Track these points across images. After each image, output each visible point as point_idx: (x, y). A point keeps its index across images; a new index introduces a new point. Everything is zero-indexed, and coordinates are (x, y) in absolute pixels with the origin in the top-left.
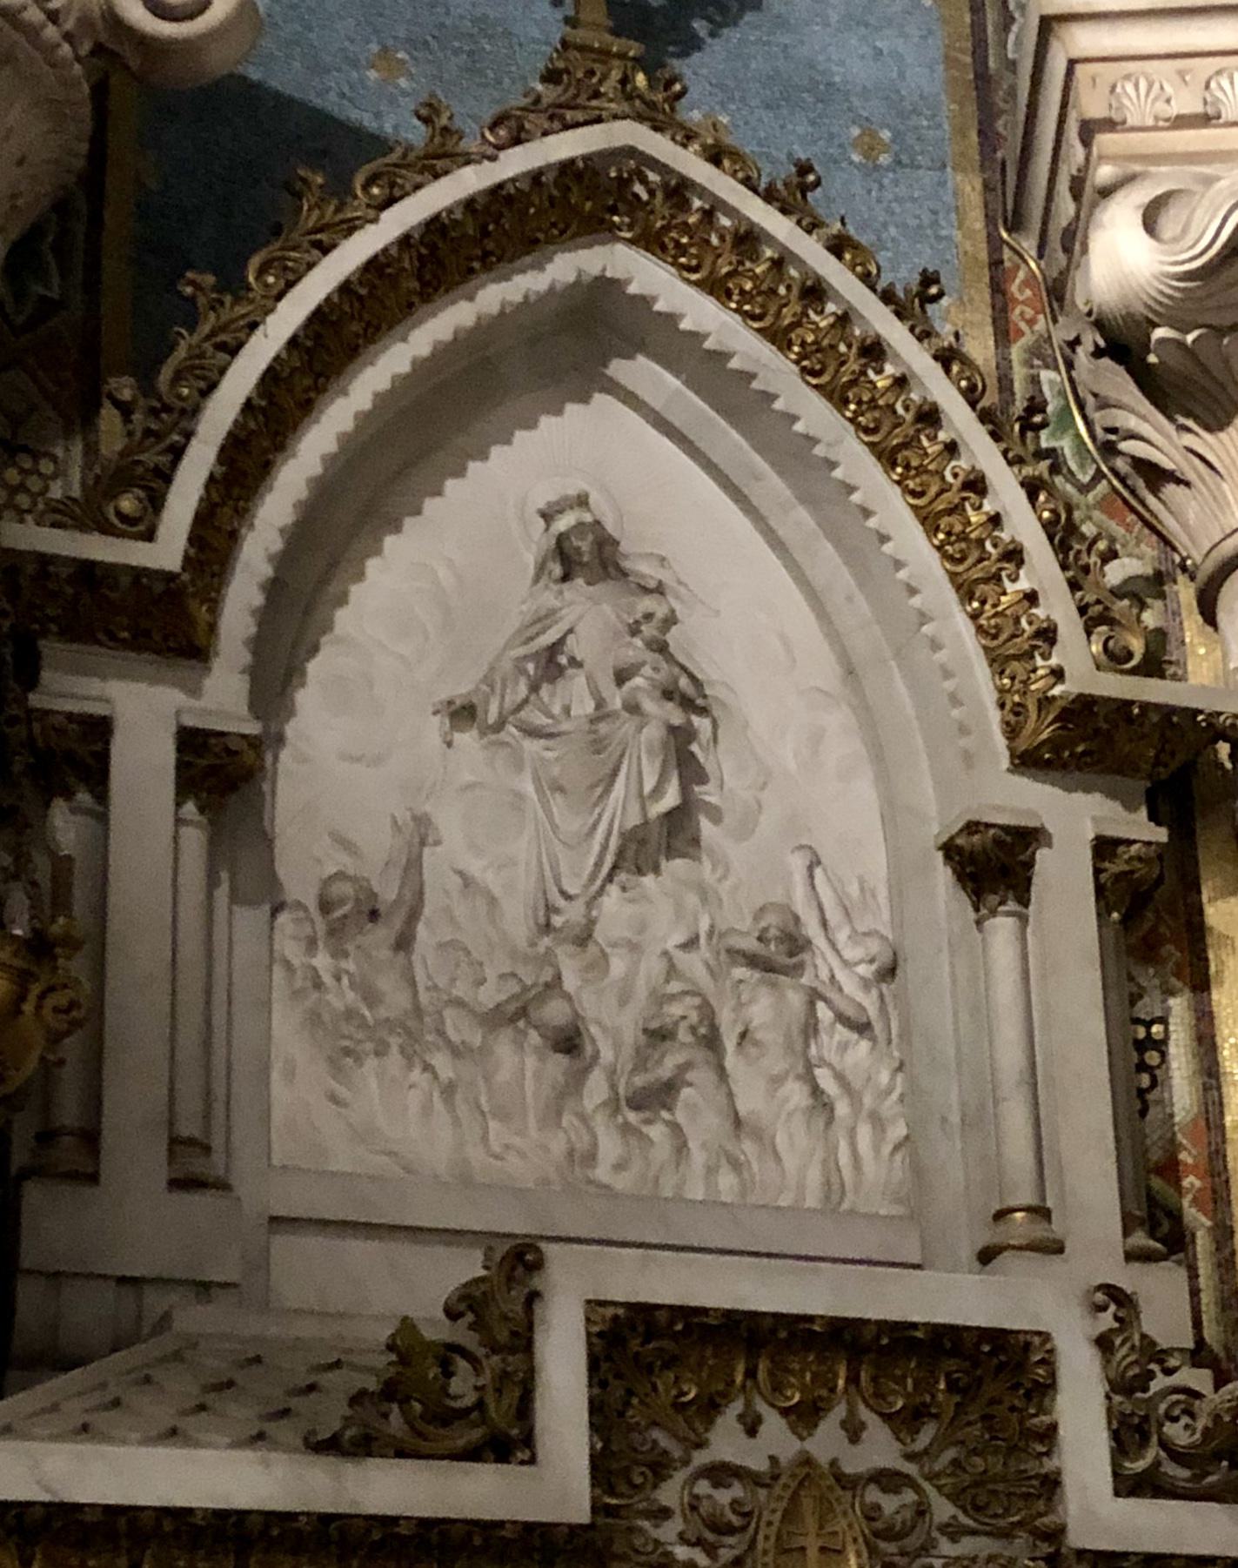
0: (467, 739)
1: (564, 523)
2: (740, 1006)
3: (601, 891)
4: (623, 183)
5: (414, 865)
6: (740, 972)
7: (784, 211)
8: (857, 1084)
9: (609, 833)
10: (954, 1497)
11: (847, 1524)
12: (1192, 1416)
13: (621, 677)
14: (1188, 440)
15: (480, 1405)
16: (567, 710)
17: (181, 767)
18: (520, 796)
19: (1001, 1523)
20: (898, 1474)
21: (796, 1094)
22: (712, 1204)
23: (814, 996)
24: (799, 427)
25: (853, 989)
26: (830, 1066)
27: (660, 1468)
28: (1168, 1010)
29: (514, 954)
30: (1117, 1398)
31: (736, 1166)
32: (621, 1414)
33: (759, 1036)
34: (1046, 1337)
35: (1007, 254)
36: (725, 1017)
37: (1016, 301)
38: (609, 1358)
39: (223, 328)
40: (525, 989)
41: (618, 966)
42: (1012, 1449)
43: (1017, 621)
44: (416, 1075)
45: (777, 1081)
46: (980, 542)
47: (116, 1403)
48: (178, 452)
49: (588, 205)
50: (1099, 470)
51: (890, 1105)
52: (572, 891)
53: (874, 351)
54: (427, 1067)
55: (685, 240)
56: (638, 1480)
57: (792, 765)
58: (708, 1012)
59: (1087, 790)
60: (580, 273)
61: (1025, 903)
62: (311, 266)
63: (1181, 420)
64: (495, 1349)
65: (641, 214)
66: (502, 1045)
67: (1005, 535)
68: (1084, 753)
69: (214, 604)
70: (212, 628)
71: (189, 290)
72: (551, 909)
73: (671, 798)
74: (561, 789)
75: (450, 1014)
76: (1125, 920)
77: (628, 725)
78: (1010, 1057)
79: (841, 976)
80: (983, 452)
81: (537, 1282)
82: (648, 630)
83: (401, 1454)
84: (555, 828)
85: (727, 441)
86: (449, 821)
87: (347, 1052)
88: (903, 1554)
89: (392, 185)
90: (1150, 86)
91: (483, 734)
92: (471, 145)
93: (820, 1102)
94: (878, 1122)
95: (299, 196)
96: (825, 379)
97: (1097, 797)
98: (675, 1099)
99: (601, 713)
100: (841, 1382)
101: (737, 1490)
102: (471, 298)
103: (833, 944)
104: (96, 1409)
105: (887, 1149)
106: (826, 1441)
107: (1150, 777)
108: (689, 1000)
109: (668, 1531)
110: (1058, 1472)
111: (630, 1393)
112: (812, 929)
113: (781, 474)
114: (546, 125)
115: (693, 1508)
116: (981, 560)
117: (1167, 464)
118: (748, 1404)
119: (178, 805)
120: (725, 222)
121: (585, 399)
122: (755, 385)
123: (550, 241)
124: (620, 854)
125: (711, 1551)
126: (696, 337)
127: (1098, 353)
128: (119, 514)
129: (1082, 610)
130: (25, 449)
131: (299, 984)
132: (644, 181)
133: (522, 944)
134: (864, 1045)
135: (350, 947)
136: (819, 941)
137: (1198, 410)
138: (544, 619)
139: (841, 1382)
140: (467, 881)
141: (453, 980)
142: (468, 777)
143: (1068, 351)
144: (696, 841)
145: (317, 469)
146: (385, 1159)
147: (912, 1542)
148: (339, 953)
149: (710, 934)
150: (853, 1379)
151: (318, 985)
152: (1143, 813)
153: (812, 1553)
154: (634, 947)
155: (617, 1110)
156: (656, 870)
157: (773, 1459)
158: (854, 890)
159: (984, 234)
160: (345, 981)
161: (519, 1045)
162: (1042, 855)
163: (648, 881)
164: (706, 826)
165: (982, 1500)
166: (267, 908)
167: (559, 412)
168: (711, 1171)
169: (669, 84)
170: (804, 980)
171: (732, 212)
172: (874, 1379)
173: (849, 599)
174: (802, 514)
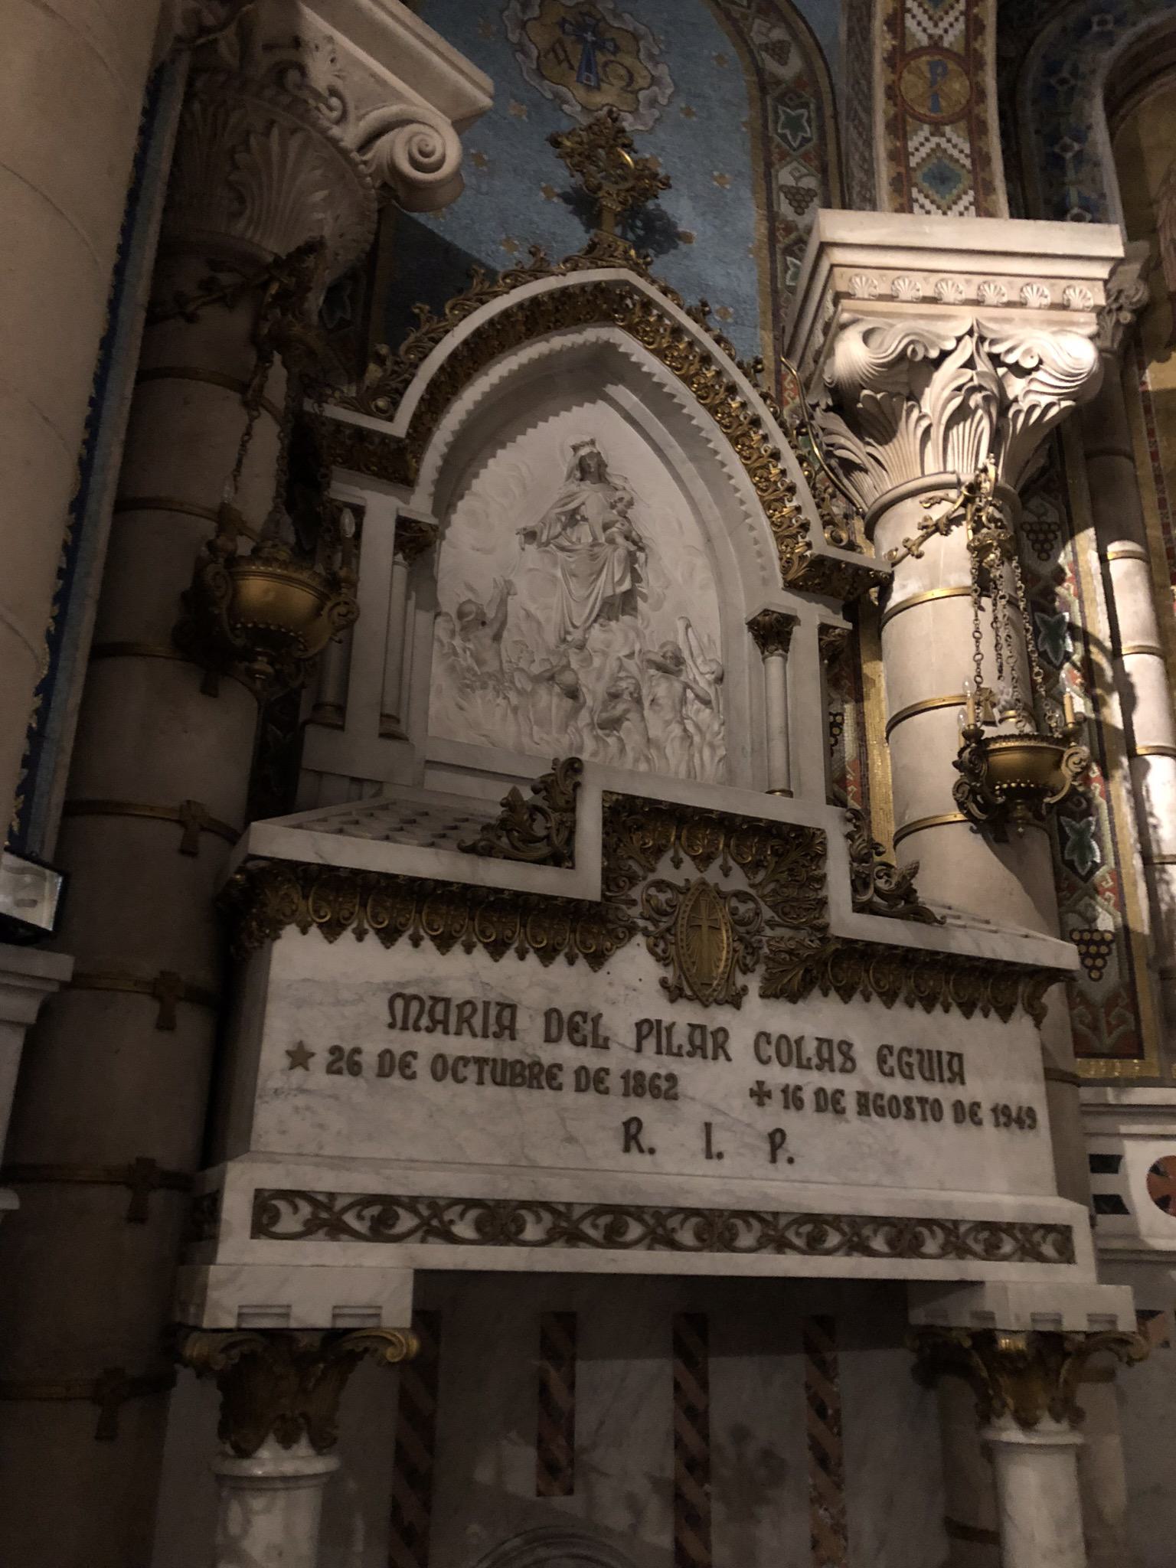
0: (532, 548)
1: (583, 452)
2: (651, 687)
3: (591, 626)
4: (622, 298)
5: (503, 603)
6: (652, 671)
7: (696, 321)
8: (704, 728)
9: (596, 599)
10: (773, 907)
11: (723, 915)
12: (889, 875)
13: (606, 527)
14: (870, 449)
15: (548, 837)
16: (579, 539)
17: (397, 536)
18: (554, 576)
19: (796, 922)
20: (746, 893)
21: (676, 730)
22: (633, 773)
23: (686, 686)
24: (694, 422)
25: (703, 684)
26: (691, 719)
27: (633, 880)
28: (844, 709)
29: (549, 651)
30: (855, 864)
31: (648, 760)
32: (615, 851)
33: (660, 701)
34: (823, 832)
35: (783, 367)
36: (644, 692)
37: (786, 389)
38: (611, 822)
39: (433, 331)
40: (553, 667)
41: (597, 662)
42: (801, 886)
43: (791, 519)
44: (500, 700)
45: (668, 723)
46: (775, 482)
47: (357, 822)
48: (407, 383)
49: (605, 306)
50: (821, 466)
51: (718, 740)
52: (577, 624)
53: (732, 390)
54: (505, 697)
55: (648, 329)
56: (622, 884)
57: (680, 579)
58: (638, 687)
59: (817, 603)
60: (598, 338)
61: (787, 651)
62: (476, 309)
63: (867, 439)
64: (555, 810)
65: (628, 315)
66: (543, 692)
67: (788, 481)
68: (819, 584)
69: (419, 460)
70: (418, 470)
71: (417, 311)
72: (568, 633)
73: (626, 585)
74: (574, 575)
75: (517, 675)
76: (829, 665)
77: (608, 549)
78: (777, 722)
79: (698, 678)
80: (780, 441)
81: (579, 779)
82: (620, 506)
83: (505, 858)
84: (570, 592)
85: (659, 429)
86: (521, 584)
87: (468, 686)
88: (748, 933)
89: (516, 280)
90: (867, 280)
91: (539, 547)
92: (554, 268)
93: (687, 735)
94: (713, 747)
95: (471, 277)
96: (708, 401)
97: (821, 606)
98: (620, 726)
99: (595, 543)
100: (721, 846)
101: (669, 895)
102: (547, 341)
103: (695, 663)
104: (345, 823)
105: (717, 759)
106: (713, 874)
107: (844, 599)
108: (630, 681)
109: (635, 912)
110: (826, 897)
111: (620, 840)
112: (686, 654)
113: (683, 445)
114: (589, 264)
115: (648, 901)
116: (775, 491)
117: (858, 461)
118: (676, 852)
119: (395, 554)
120: (667, 322)
121: (593, 402)
122: (676, 400)
123: (586, 321)
124: (601, 611)
125: (656, 923)
126: (650, 375)
127: (828, 409)
128: (377, 407)
129: (822, 516)
130: (328, 385)
131: (446, 650)
132: (631, 298)
133: (552, 646)
134: (708, 711)
135: (471, 637)
136: (689, 662)
137: (875, 433)
138: (571, 496)
139: (721, 846)
140: (529, 615)
141: (520, 658)
142: (532, 567)
143: (810, 410)
144: (635, 609)
145: (471, 407)
146: (483, 738)
147: (751, 928)
148: (466, 639)
149: (640, 651)
150: (727, 845)
151: (455, 654)
152: (841, 616)
153: (705, 929)
154: (605, 654)
155: (593, 728)
156: (617, 620)
157: (687, 880)
158: (705, 640)
159: (773, 358)
160: (468, 653)
161: (550, 693)
162: (795, 629)
163: (613, 623)
164: (640, 601)
165: (787, 910)
166: (433, 614)
167: (581, 405)
168: (636, 760)
169: (645, 257)
170: (682, 678)
171: (671, 317)
172: (737, 846)
173: (710, 507)
174: (690, 466)
